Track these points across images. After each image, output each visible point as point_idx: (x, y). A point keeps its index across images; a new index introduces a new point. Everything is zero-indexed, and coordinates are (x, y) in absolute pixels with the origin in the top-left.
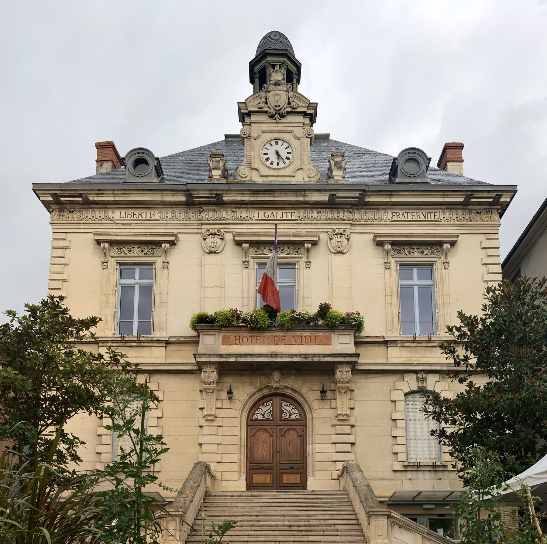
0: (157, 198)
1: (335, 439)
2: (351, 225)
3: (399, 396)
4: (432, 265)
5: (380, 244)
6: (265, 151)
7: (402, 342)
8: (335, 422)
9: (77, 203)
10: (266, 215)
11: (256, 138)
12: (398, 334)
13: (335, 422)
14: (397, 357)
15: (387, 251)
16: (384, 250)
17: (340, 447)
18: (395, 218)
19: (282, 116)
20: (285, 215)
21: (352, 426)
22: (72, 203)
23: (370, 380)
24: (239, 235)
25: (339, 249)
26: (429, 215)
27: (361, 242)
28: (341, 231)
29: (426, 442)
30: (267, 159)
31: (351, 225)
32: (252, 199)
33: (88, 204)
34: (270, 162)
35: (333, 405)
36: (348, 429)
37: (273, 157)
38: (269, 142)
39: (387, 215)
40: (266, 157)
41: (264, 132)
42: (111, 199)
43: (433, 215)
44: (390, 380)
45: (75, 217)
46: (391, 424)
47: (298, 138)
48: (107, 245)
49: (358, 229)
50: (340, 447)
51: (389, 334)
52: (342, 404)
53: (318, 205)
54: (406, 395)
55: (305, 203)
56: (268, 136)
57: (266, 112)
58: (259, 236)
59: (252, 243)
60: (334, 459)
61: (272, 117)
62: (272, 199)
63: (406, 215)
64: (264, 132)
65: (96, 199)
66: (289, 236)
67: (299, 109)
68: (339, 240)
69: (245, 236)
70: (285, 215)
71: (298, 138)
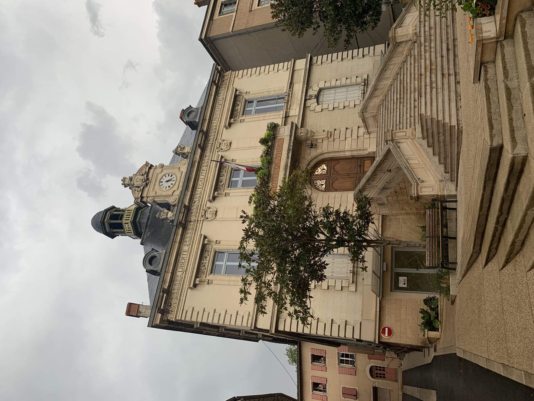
0: (177, 245)
1: (342, 138)
2: (216, 140)
3: (319, 108)
4: (246, 100)
5: (230, 125)
7: (287, 109)
8: (332, 139)
9: (166, 299)
12: (282, 112)
13: (332, 139)
14: (295, 111)
15: (235, 121)
16: (234, 123)
17: (349, 135)
21: (335, 130)
22: (165, 303)
23: (307, 124)
24: (209, 196)
25: (229, 144)
27: (227, 135)
28: (218, 144)
29: (348, 93)
31: (216, 140)
32: (190, 190)
33: (168, 292)
35: (321, 141)
36: (337, 132)
39: (215, 123)
42: (170, 274)
44: (308, 113)
45: (174, 301)
46: (336, 110)
48: (198, 279)
49: (219, 137)
50: (349, 135)
52: (320, 135)
53: (202, 156)
54: (318, 104)
55: (199, 163)
58: (212, 185)
59: (216, 189)
60: (356, 138)
62: (193, 179)
65: (167, 285)
66: (216, 169)
69: (210, 193)
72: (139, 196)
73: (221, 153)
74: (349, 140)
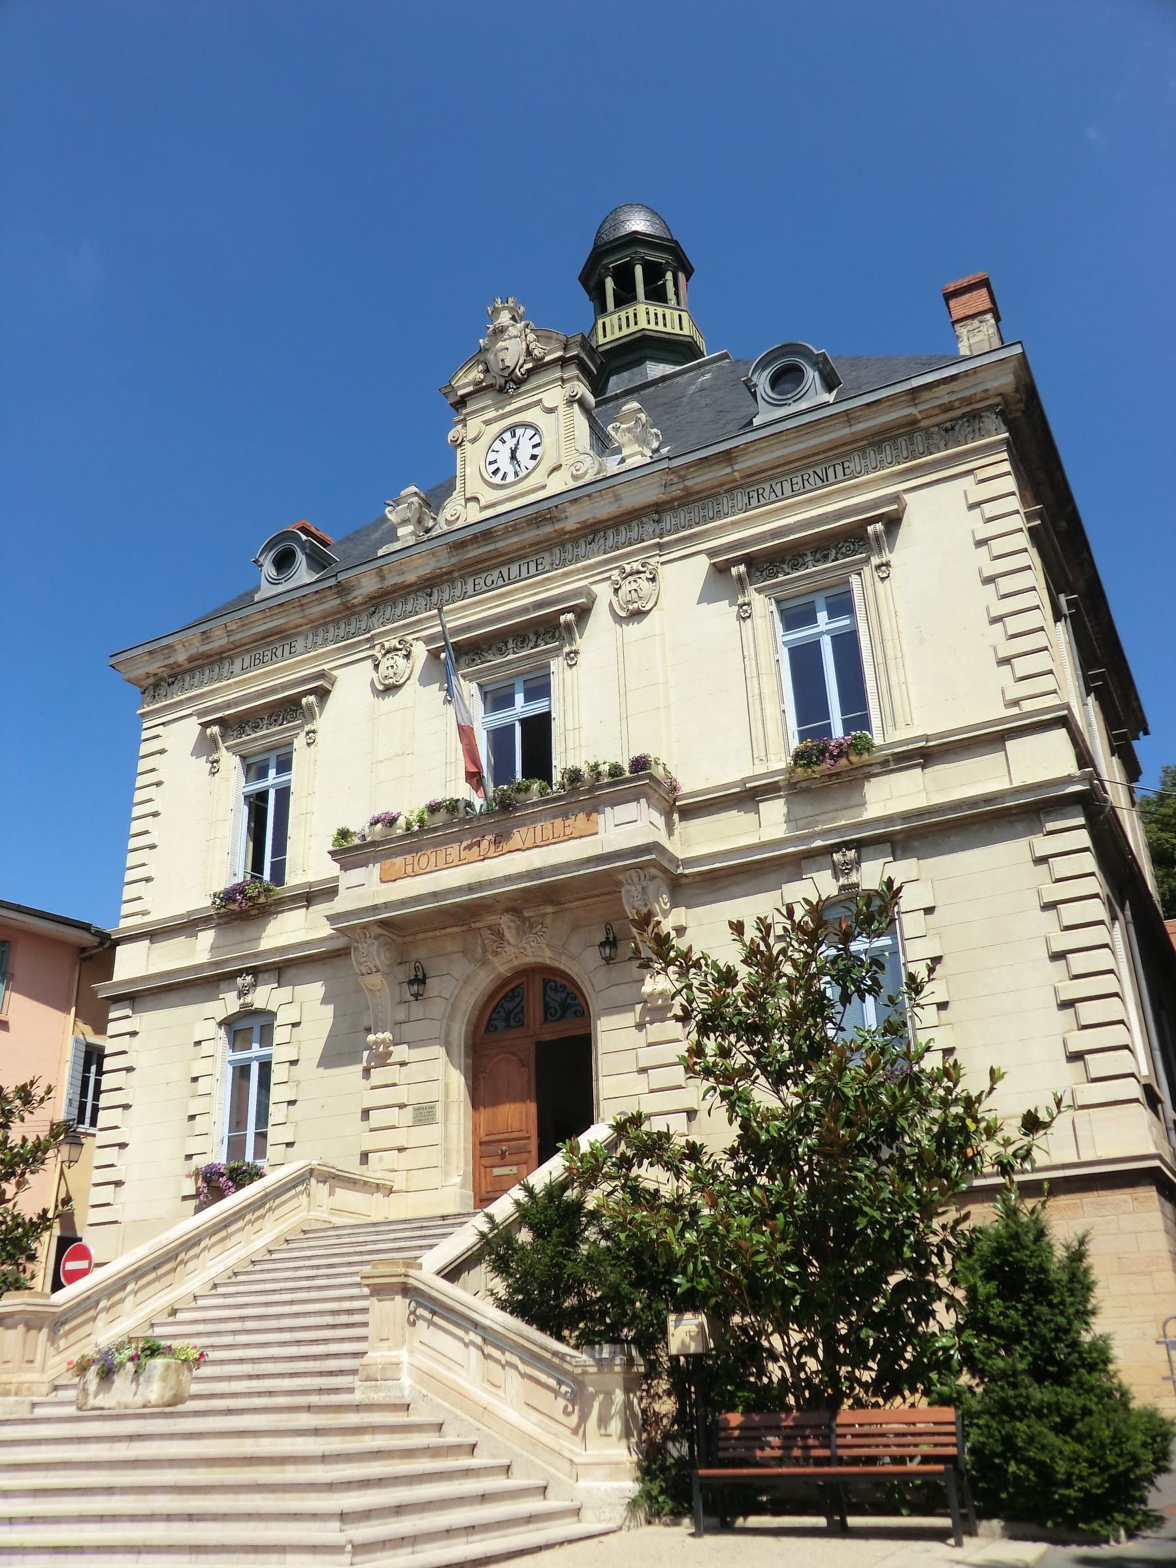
6: (492, 457)
10: (489, 582)
11: (474, 440)
18: (754, 502)
19: (520, 382)
20: (524, 569)
26: (831, 471)
30: (495, 472)
31: (660, 546)
34: (500, 475)
37: (505, 465)
38: (499, 437)
40: (493, 467)
41: (488, 423)
43: (839, 469)
47: (551, 411)
51: (761, 769)
56: (497, 427)
57: (491, 386)
61: (502, 390)
63: (778, 489)
64: (488, 423)
67: (547, 359)
68: (634, 586)
70: (524, 569)
71: (551, 411)
72: (460, 392)
73: (603, 592)
74: (640, 1083)
